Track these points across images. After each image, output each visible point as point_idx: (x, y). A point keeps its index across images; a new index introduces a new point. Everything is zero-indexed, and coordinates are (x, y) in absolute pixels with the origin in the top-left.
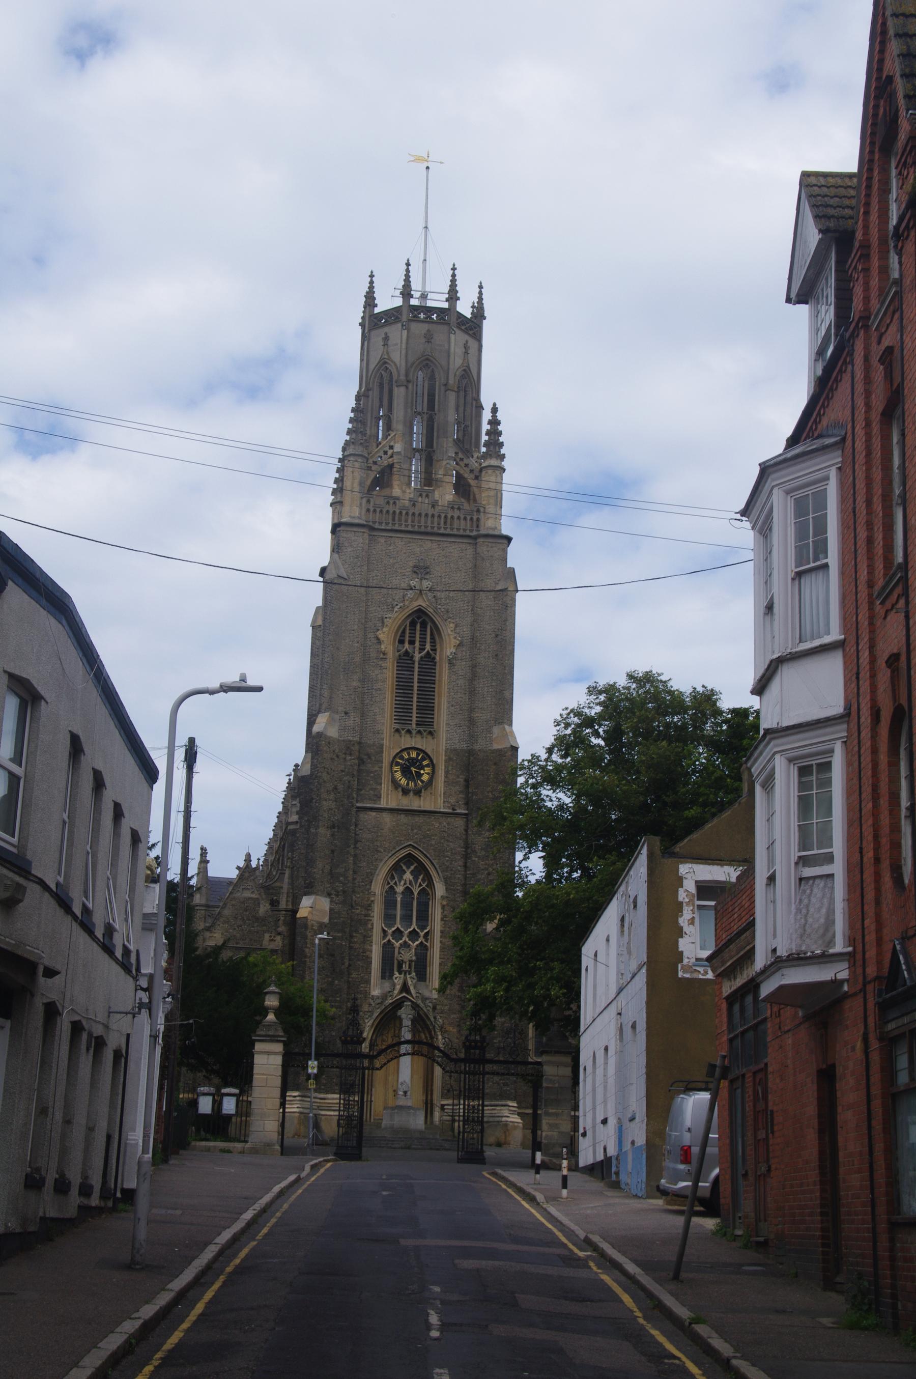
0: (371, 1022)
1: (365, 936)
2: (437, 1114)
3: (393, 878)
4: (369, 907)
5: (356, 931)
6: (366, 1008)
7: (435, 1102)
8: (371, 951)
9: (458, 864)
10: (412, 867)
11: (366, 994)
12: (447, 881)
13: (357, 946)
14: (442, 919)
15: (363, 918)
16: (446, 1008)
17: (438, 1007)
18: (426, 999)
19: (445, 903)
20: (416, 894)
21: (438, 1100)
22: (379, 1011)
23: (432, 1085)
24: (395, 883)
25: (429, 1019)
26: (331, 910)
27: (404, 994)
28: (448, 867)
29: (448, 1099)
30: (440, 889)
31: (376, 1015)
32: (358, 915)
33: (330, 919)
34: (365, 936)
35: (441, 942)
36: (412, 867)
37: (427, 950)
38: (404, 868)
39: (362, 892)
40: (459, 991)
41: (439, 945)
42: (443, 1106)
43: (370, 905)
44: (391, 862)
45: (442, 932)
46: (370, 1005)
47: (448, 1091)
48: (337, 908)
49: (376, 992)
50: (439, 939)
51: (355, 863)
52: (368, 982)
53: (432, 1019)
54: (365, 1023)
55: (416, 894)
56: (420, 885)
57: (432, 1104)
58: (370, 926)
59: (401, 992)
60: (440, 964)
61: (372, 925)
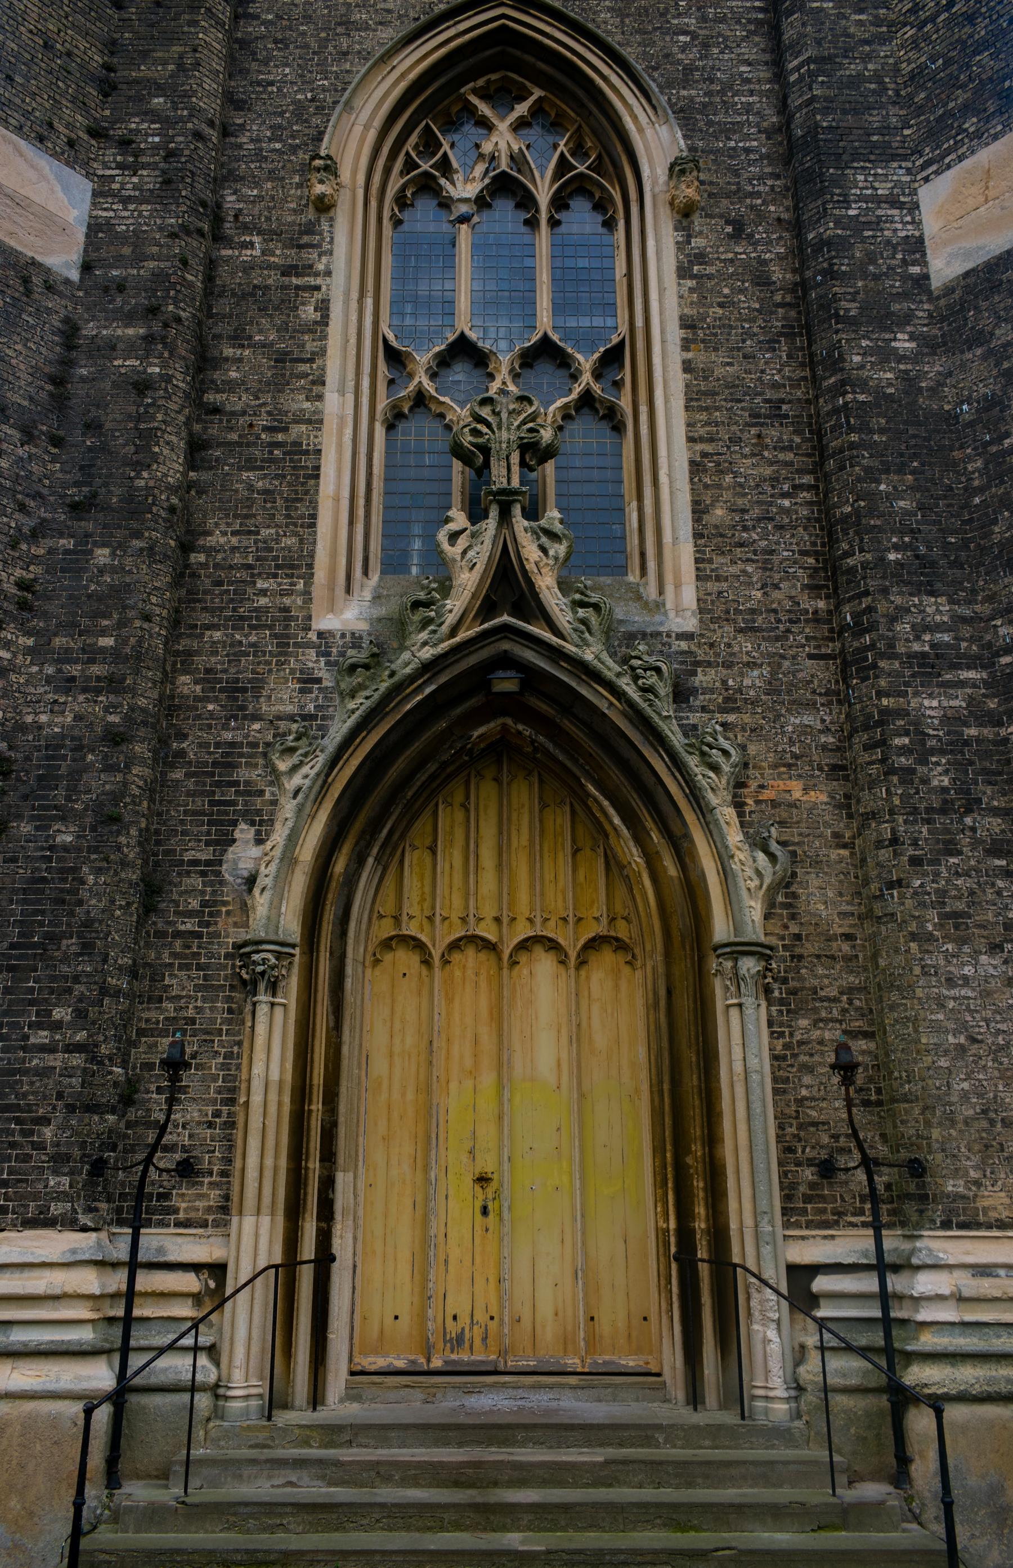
0: (311, 769)
1: (282, 359)
2: (769, 1333)
3: (429, 144)
4: (306, 236)
5: (239, 338)
6: (282, 698)
7: (743, 1250)
8: (316, 422)
9: (743, 58)
10: (522, 109)
11: (287, 628)
12: (686, 117)
13: (236, 402)
14: (683, 272)
15: (273, 279)
16: (754, 679)
17: (702, 678)
18: (631, 638)
19: (689, 192)
20: (543, 196)
21: (764, 1241)
22: (360, 704)
23: (712, 1139)
24: (445, 166)
25: (659, 740)
26: (95, 228)
27: (506, 618)
28: (689, 70)
29: (829, 1222)
30: (656, 142)
31: (338, 730)
32: (248, 268)
33: (86, 268)
34: (282, 359)
35: (687, 367)
36: (522, 109)
37: (618, 428)
38: (484, 108)
39: (272, 175)
40: (814, 589)
41: (678, 380)
42: (801, 1275)
43: (310, 229)
44: (412, 63)
45: (687, 324)
46: (308, 681)
47: (827, 1169)
48: (126, 219)
49: (346, 615)
50: (676, 357)
51: (234, 67)
52: (298, 565)
53: (677, 739)
54: (275, 777)
55: (543, 196)
56: (563, 166)
57: (725, 1270)
58: (309, 313)
59: (487, 607)
60: (696, 467)
61: (324, 307)
